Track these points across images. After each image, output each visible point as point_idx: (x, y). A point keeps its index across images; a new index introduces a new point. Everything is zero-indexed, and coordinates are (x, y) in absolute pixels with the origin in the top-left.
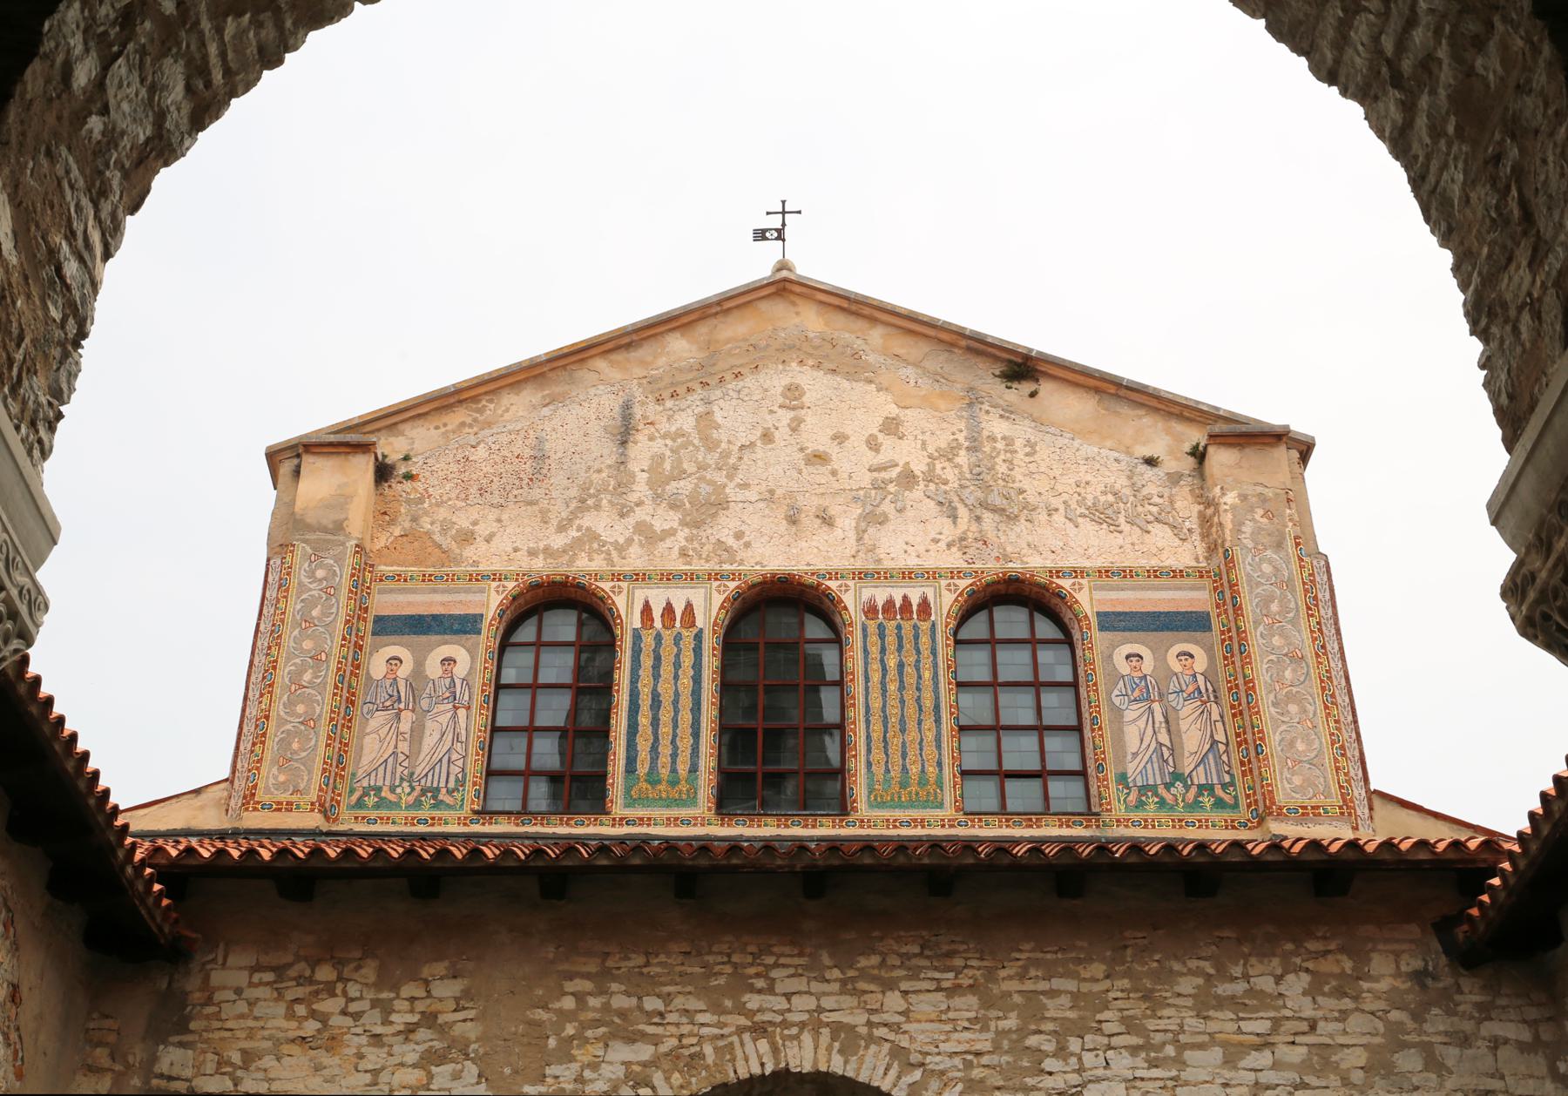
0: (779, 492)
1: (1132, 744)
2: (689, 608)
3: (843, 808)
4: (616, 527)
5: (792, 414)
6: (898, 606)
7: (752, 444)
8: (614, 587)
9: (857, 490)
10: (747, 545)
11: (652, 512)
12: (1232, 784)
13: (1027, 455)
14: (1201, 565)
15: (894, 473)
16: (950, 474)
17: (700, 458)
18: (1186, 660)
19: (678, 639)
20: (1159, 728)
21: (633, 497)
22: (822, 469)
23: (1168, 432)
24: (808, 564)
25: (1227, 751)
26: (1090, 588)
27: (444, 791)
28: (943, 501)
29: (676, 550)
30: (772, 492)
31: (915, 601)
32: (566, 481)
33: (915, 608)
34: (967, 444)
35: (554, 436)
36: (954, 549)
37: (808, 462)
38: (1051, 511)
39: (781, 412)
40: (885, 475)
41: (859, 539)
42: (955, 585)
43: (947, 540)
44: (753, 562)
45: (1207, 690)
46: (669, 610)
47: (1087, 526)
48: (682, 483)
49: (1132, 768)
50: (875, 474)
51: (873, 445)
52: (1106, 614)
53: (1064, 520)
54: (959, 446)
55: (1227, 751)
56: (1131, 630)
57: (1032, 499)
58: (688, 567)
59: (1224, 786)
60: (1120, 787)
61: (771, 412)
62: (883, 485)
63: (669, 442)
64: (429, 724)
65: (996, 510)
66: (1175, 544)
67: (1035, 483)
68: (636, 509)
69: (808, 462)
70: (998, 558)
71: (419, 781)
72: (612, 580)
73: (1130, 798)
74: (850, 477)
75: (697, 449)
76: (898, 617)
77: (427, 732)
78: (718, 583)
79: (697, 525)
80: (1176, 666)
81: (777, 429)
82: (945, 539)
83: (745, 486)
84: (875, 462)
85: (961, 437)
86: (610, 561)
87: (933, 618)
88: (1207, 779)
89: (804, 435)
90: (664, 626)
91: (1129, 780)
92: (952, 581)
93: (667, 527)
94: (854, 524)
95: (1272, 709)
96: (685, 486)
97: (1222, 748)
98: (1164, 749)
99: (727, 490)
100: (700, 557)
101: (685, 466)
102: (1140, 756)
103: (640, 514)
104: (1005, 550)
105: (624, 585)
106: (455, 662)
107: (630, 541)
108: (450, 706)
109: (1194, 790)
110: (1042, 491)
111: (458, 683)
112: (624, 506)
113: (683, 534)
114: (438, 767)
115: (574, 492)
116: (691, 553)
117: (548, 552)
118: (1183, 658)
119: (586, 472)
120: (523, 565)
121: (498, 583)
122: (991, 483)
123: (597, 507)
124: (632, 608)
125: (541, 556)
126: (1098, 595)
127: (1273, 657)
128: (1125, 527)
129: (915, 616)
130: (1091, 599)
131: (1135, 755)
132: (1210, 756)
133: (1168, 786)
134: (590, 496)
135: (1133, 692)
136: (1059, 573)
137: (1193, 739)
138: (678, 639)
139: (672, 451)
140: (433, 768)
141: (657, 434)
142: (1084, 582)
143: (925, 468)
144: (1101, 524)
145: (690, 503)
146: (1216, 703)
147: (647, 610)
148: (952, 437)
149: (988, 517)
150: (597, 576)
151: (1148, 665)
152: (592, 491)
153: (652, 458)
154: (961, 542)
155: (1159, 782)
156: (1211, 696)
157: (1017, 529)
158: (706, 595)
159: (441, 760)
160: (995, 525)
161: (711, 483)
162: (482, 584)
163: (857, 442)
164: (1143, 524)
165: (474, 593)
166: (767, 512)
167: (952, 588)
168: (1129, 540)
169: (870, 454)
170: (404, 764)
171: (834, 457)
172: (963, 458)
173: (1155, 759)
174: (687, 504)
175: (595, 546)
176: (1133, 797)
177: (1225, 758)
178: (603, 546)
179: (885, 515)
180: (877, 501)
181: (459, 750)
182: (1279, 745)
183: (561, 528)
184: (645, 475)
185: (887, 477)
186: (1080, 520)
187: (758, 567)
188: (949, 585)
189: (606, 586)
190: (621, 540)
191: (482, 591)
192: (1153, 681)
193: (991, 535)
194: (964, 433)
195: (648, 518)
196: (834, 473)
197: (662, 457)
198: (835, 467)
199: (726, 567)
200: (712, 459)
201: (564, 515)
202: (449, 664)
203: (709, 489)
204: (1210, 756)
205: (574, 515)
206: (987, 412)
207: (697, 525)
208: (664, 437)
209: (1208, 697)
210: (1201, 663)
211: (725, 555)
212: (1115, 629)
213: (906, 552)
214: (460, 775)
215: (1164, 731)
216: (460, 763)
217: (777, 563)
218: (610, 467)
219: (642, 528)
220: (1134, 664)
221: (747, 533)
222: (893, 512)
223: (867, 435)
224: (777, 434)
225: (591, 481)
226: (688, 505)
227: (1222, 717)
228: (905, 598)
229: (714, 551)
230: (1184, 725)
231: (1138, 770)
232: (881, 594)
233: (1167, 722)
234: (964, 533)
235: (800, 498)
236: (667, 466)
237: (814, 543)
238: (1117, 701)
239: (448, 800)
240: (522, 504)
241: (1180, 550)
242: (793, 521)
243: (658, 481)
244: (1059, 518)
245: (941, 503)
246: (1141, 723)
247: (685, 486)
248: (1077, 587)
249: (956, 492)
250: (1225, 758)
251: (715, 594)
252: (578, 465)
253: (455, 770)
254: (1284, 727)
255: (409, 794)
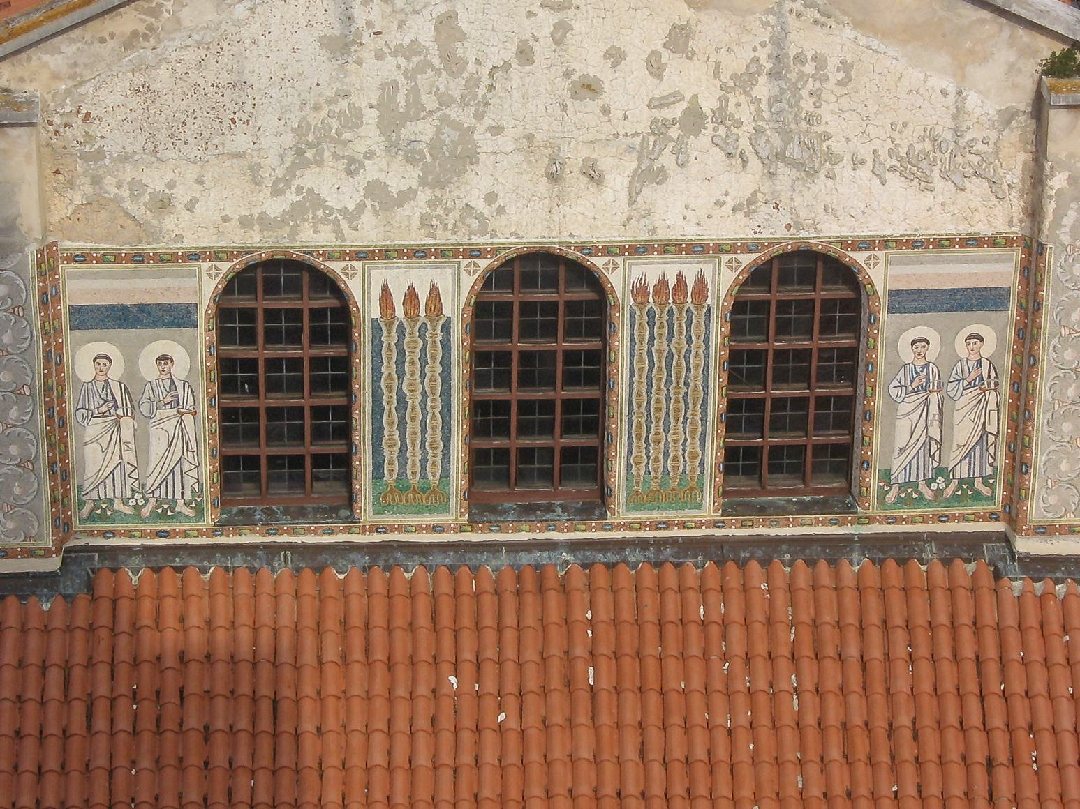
0: (541, 137)
1: (902, 439)
2: (434, 290)
3: (597, 504)
4: (343, 189)
5: (556, 17)
6: (671, 286)
7: (507, 66)
8: (346, 268)
9: (633, 136)
10: (501, 210)
11: (386, 168)
12: (993, 476)
13: (839, 83)
14: (1013, 229)
15: (677, 111)
16: (745, 114)
17: (442, 89)
18: (975, 343)
19: (423, 331)
20: (932, 421)
21: (360, 147)
22: (593, 106)
23: (1012, 42)
24: (571, 235)
25: (995, 443)
26: (886, 261)
27: (181, 502)
28: (733, 152)
29: (416, 222)
30: (529, 138)
31: (691, 281)
32: (277, 123)
33: (690, 290)
34: (768, 66)
35: (255, 53)
36: (740, 215)
37: (575, 95)
38: (857, 163)
39: (542, 13)
40: (668, 114)
41: (632, 202)
42: (737, 261)
43: (733, 203)
44: (507, 232)
45: (989, 376)
46: (411, 294)
47: (895, 181)
48: (421, 124)
49: (897, 466)
50: (656, 113)
51: (655, 67)
52: (899, 293)
53: (869, 174)
54: (761, 68)
55: (995, 443)
56: (922, 311)
57: (837, 146)
58: (432, 241)
59: (985, 481)
60: (882, 484)
61: (530, 14)
62: (663, 130)
63: (401, 61)
64: (153, 431)
65: (796, 164)
66: (990, 204)
67: (844, 125)
68: (367, 162)
69: (575, 95)
70: (788, 227)
71: (152, 492)
72: (345, 260)
73: (890, 495)
74: (625, 117)
75: (438, 73)
76: (671, 300)
77: (154, 441)
78: (467, 261)
79: (440, 184)
80: (961, 349)
81: (537, 40)
82: (730, 202)
83: (496, 130)
84: (657, 94)
85: (763, 55)
86: (339, 233)
87: (709, 302)
88: (969, 472)
89: (571, 49)
90: (406, 314)
91: (892, 477)
92: (734, 256)
93: (405, 188)
94: (626, 184)
95: (1046, 428)
96: (423, 130)
97: (991, 439)
98: (933, 443)
99: (476, 137)
100: (445, 227)
101: (424, 98)
102: (908, 451)
103: (372, 171)
104: (798, 216)
105: (358, 264)
106: (172, 361)
107: (360, 207)
108: (174, 411)
109: (954, 484)
110: (851, 136)
111: (179, 385)
112: (351, 160)
113: (424, 196)
114: (170, 478)
115: (289, 139)
116: (434, 222)
117: (263, 220)
118: (971, 341)
119: (301, 110)
120: (237, 239)
121: (210, 264)
122: (793, 126)
123: (319, 162)
124: (369, 293)
125: (256, 227)
126: (893, 270)
127: (1060, 373)
128: (939, 183)
129: (689, 300)
130: (886, 275)
131: (902, 450)
132: (978, 449)
133: (928, 483)
134: (310, 146)
135: (912, 382)
136: (856, 245)
137: (964, 431)
138: (423, 331)
139: (405, 75)
140: (166, 479)
141: (385, 49)
142: (881, 254)
143: (716, 105)
144: (912, 180)
145: (431, 155)
146: (996, 391)
147: (386, 295)
148: (752, 55)
149: (785, 175)
150: (328, 255)
151: (932, 353)
152: (310, 138)
153: (382, 86)
154: (748, 206)
155: (921, 478)
156: (992, 383)
157: (814, 188)
158: (453, 276)
159: (172, 470)
160: (790, 182)
161: (457, 126)
162: (191, 265)
163: (635, 63)
164: (957, 178)
165: (183, 277)
166: (525, 166)
167: (734, 264)
168: (940, 199)
169: (652, 80)
170: (135, 475)
171: (606, 87)
172: (763, 88)
173: (921, 452)
174: (428, 156)
175: (320, 213)
176: (891, 496)
177: (991, 450)
178: (330, 214)
179: (662, 170)
180: (656, 154)
181: (191, 459)
182: (1044, 465)
183: (277, 192)
184: (374, 113)
185: (670, 117)
186: (889, 175)
187: (513, 240)
188: (730, 261)
189: (336, 267)
190: (351, 207)
191: (191, 274)
192: (935, 370)
193: (784, 197)
194: (768, 49)
195: (382, 178)
196: (606, 111)
197: (394, 85)
198: (608, 101)
199: (477, 240)
200: (456, 88)
201: (280, 173)
202: (165, 364)
203: (455, 135)
204: (978, 449)
205: (291, 171)
206: (799, 15)
207: (440, 184)
208: (395, 54)
209: (989, 385)
210: (988, 349)
211: (475, 224)
212: (905, 310)
213: (685, 218)
214: (196, 487)
215: (936, 423)
216: (194, 473)
217: (535, 233)
218: (329, 101)
219: (375, 190)
220: (918, 350)
221: (501, 195)
222: (674, 164)
223: (649, 51)
224: (536, 49)
225: (309, 125)
226: (428, 159)
227: (998, 406)
228: (680, 275)
229: (462, 219)
230: (957, 416)
231: (904, 465)
232: (652, 271)
233: (941, 414)
234: (754, 194)
235: (564, 148)
236: (401, 98)
237: (580, 209)
238: (893, 392)
239: (188, 511)
240: (225, 157)
241: (996, 211)
242: (554, 177)
243: (391, 123)
244: (864, 173)
245: (729, 155)
246: (915, 416)
247: (423, 130)
248: (872, 262)
249: (750, 139)
250: (991, 450)
251: (463, 274)
252: (290, 98)
253: (190, 481)
254: (1053, 447)
255: (144, 506)
